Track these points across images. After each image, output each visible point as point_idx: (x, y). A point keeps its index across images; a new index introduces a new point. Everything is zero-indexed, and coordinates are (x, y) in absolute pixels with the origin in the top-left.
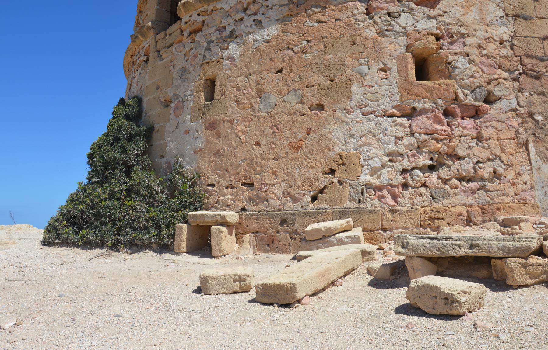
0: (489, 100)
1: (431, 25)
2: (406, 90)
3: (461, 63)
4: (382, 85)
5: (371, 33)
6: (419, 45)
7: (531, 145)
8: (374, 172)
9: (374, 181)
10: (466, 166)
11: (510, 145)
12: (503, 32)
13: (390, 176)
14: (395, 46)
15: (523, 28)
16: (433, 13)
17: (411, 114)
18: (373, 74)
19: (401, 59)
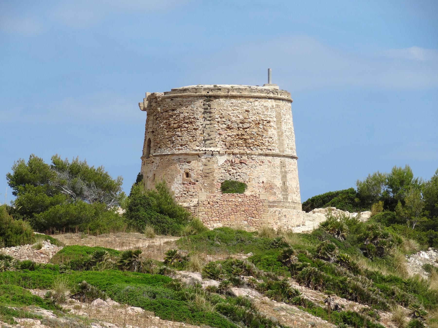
0: (197, 181)
1: (189, 167)
2: (183, 179)
3: (192, 175)
4: (179, 178)
5: (179, 169)
6: (186, 171)
7: (203, 189)
8: (177, 194)
9: (177, 196)
10: (191, 193)
11: (199, 189)
12: (201, 168)
13: (179, 195)
14: (182, 171)
15: (205, 167)
16: (189, 164)
17: (184, 184)
18: (179, 177)
19: (183, 174)
